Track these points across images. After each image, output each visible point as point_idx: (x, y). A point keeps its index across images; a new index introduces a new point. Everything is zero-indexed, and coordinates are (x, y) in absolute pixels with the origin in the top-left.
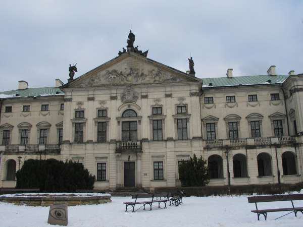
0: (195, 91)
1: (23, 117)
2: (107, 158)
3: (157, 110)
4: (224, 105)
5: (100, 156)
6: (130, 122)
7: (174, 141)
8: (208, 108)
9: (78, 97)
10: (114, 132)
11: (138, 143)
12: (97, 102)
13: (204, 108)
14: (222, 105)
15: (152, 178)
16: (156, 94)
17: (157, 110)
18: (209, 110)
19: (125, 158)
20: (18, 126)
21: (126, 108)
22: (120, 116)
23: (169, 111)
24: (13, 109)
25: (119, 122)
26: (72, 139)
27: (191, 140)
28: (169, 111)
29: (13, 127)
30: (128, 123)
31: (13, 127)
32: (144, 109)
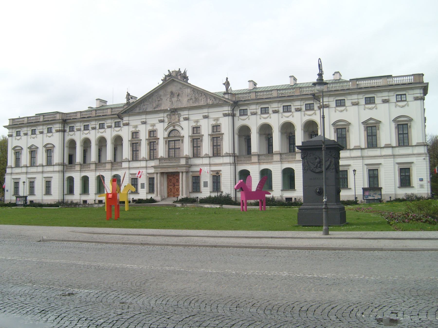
0: (227, 112)
3: (196, 129)
6: (175, 141)
7: (210, 157)
9: (135, 121)
10: (162, 150)
12: (149, 125)
16: (196, 116)
17: (196, 129)
21: (171, 128)
23: (206, 130)
25: (166, 142)
26: (130, 158)
28: (206, 130)
30: (173, 142)
32: (185, 129)
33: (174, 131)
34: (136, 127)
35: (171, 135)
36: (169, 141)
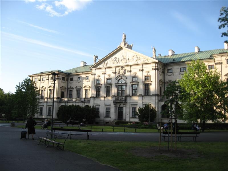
1: (78, 83)
2: (110, 105)
4: (179, 73)
5: (107, 104)
8: (169, 76)
10: (114, 91)
11: (124, 97)
13: (167, 75)
14: (177, 74)
15: (131, 116)
18: (169, 77)
19: (118, 105)
20: (76, 88)
21: (120, 78)
22: (116, 82)
24: (73, 79)
25: (116, 86)
27: (151, 96)
29: (73, 88)
31: (73, 88)
33: (120, 80)
34: (99, 76)
35: (120, 82)
36: (118, 86)
